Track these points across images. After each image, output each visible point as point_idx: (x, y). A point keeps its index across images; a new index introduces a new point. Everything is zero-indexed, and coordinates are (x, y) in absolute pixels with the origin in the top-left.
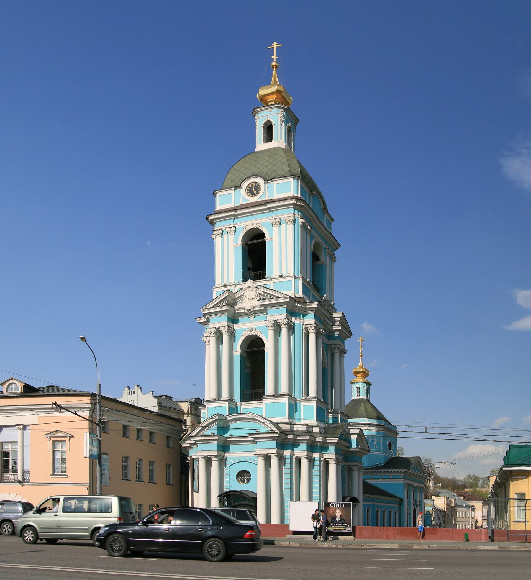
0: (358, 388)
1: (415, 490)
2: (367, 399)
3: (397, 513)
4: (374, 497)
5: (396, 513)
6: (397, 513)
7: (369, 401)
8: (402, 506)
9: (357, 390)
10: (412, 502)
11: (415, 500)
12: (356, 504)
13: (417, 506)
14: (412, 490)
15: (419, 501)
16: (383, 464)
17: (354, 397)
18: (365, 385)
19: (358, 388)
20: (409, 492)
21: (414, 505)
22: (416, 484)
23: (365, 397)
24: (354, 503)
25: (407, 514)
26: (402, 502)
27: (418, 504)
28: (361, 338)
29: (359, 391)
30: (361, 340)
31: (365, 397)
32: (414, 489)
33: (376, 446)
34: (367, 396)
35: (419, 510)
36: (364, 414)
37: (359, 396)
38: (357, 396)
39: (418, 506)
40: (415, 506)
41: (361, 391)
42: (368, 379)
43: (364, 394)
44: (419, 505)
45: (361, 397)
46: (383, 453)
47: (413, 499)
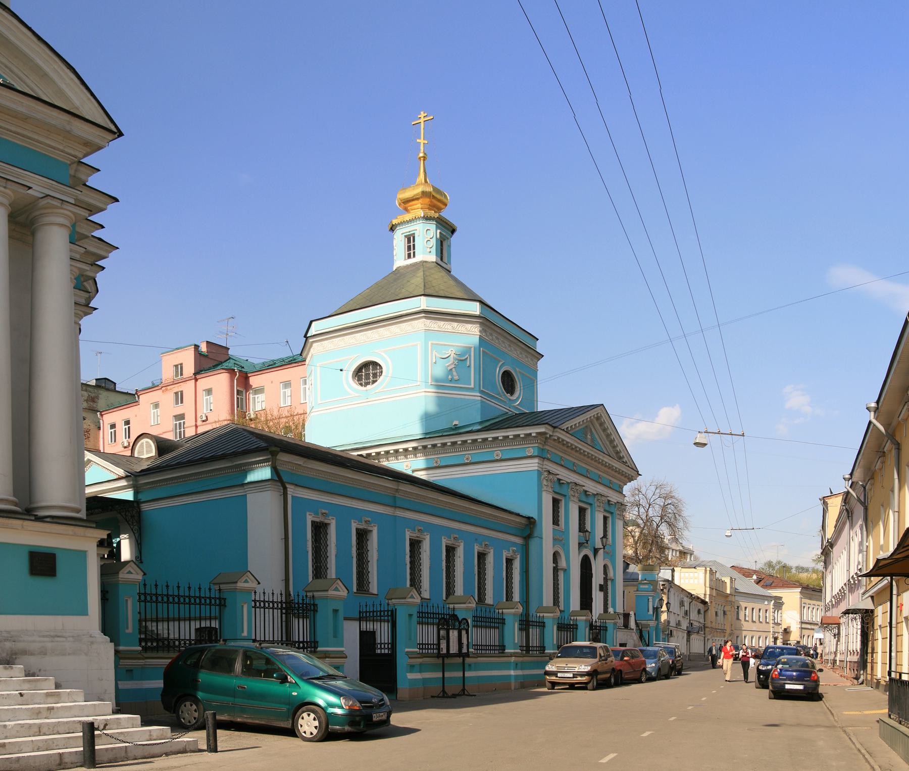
0: (410, 239)
3: (517, 565)
4: (397, 490)
5: (509, 561)
7: (450, 272)
8: (533, 543)
9: (409, 241)
13: (596, 551)
14: (576, 500)
15: (605, 536)
17: (400, 261)
18: (432, 226)
19: (410, 239)
20: (562, 505)
21: (580, 545)
22: (592, 487)
28: (422, 114)
29: (414, 245)
30: (422, 120)
31: (432, 258)
33: (455, 373)
37: (414, 256)
38: (409, 256)
39: (601, 552)
41: (419, 243)
42: (446, 214)
43: (429, 250)
45: (419, 258)
46: (479, 394)
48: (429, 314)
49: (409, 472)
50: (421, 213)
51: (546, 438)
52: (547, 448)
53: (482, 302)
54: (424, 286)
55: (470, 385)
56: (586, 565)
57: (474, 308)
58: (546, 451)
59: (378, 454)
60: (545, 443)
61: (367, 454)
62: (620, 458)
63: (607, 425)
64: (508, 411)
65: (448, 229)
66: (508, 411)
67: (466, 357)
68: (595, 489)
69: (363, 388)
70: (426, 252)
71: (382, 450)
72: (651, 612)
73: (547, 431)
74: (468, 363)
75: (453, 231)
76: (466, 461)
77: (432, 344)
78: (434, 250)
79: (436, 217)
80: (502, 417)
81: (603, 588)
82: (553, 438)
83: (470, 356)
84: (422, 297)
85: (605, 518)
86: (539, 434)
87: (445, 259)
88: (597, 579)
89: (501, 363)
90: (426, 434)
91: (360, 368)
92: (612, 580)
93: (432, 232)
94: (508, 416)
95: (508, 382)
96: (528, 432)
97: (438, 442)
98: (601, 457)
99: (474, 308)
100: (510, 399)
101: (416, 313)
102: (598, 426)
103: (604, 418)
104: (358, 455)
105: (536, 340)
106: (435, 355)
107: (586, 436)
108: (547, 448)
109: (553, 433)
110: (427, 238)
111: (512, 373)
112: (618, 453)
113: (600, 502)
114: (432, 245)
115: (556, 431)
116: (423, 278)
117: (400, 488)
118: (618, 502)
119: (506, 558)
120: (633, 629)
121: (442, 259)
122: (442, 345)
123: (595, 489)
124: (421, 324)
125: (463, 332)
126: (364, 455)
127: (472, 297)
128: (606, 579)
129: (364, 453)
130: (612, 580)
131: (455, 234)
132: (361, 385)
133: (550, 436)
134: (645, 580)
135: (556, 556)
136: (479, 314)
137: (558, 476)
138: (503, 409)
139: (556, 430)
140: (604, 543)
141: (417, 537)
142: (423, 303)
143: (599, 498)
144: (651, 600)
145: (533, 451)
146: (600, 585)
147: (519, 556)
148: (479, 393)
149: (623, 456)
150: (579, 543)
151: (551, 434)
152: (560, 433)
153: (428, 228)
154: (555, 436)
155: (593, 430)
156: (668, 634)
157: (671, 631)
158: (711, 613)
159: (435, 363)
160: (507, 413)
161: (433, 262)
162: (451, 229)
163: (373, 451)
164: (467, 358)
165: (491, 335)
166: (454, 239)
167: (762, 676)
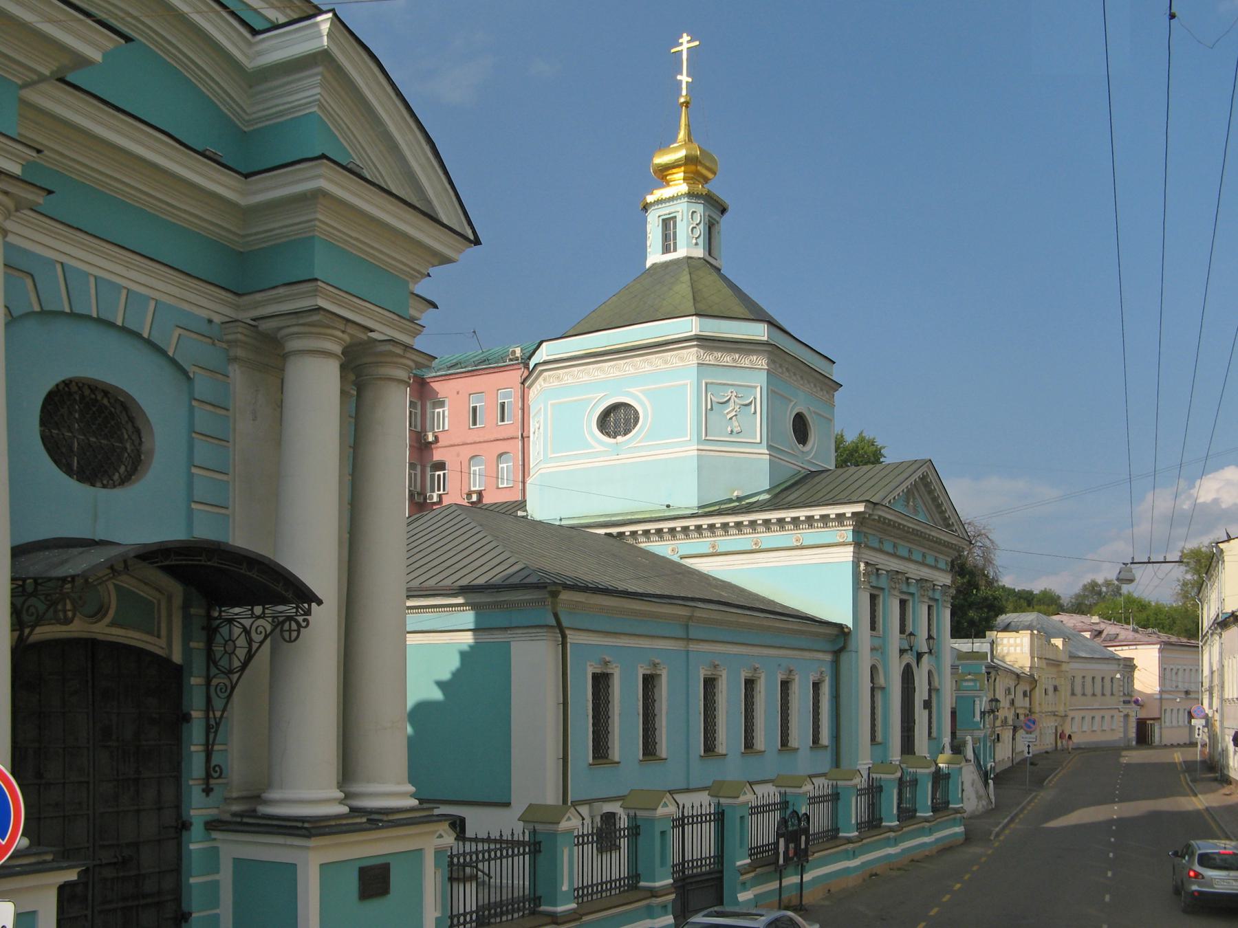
0: (668, 224)
1: (912, 594)
2: (705, 260)
3: (826, 690)
4: (690, 618)
5: (816, 686)
6: (826, 690)
8: (844, 657)
10: (895, 640)
11: (907, 633)
12: (290, 619)
13: (919, 656)
14: (896, 593)
15: (930, 637)
16: (766, 496)
17: (655, 256)
19: (668, 224)
23: (699, 252)
24: (281, 608)
25: (873, 689)
26: (846, 641)
27: (925, 649)
31: (699, 252)
32: (904, 588)
34: (710, 248)
35: (930, 673)
36: (689, 306)
37: (675, 250)
39: (925, 658)
40: (909, 658)
41: (682, 230)
42: (716, 187)
44: (930, 652)
45: (681, 253)
47: (902, 631)
48: (705, 342)
49: (676, 558)
50: (684, 188)
51: (864, 518)
52: (865, 530)
53: (772, 323)
54: (694, 299)
55: (756, 438)
56: (908, 676)
57: (759, 332)
58: (863, 534)
59: (634, 533)
60: (862, 524)
61: (618, 533)
62: (948, 526)
63: (935, 485)
64: (801, 469)
65: (716, 208)
66: (801, 469)
67: (750, 400)
68: (918, 572)
69: (612, 440)
70: (688, 246)
71: (640, 528)
72: (978, 718)
73: (867, 511)
74: (753, 410)
75: (723, 211)
76: (754, 547)
77: (706, 384)
78: (701, 241)
79: (704, 194)
80: (794, 478)
81: (927, 705)
82: (873, 517)
83: (755, 399)
84: (694, 318)
85: (930, 607)
86: (854, 514)
87: (715, 253)
88: (921, 694)
89: (793, 403)
90: (699, 507)
91: (608, 411)
92: (938, 690)
93: (699, 215)
94: (801, 476)
95: (801, 428)
96: (841, 512)
97: (717, 521)
98: (928, 532)
99: (759, 332)
100: (803, 452)
101: (686, 340)
102: (923, 488)
103: (932, 477)
104: (606, 534)
105: (831, 364)
106: (711, 399)
107: (908, 503)
108: (865, 530)
109: (873, 511)
110: (692, 224)
111: (805, 416)
112: (945, 519)
113: (924, 590)
114: (699, 233)
115: (879, 509)
116: (689, 284)
117: (695, 614)
118: (944, 585)
119: (813, 683)
120: (970, 761)
121: (710, 254)
122: (720, 384)
123: (918, 572)
124: (691, 356)
125: (746, 366)
126: (615, 534)
127: (759, 315)
128: (930, 691)
129: (614, 531)
130: (938, 690)
131: (727, 215)
132: (608, 435)
133: (870, 515)
134: (969, 675)
135: (874, 669)
136: (766, 339)
137: (877, 566)
138: (795, 467)
139: (877, 507)
140: (931, 645)
141: (712, 674)
142: (691, 326)
143: (923, 585)
144: (977, 702)
145: (845, 535)
146: (924, 701)
147: (827, 678)
148: (767, 449)
149: (953, 523)
150: (900, 650)
151: (871, 512)
152: (883, 510)
153: (694, 210)
154: (876, 515)
155: (916, 493)
156: (994, 740)
157: (998, 735)
158: (1038, 693)
159: (712, 409)
160: (800, 471)
161: (700, 258)
162: (722, 208)
163: (627, 530)
164: (752, 401)
165: (781, 366)
166: (725, 222)
167: (1117, 800)
